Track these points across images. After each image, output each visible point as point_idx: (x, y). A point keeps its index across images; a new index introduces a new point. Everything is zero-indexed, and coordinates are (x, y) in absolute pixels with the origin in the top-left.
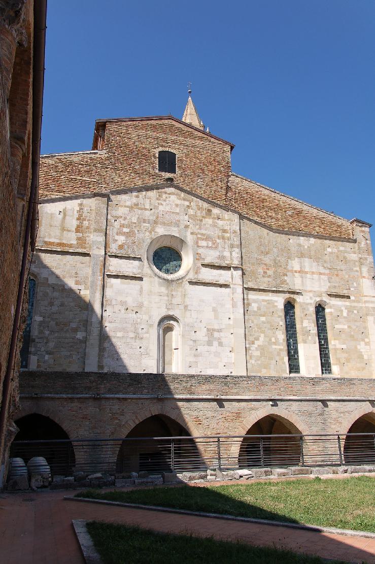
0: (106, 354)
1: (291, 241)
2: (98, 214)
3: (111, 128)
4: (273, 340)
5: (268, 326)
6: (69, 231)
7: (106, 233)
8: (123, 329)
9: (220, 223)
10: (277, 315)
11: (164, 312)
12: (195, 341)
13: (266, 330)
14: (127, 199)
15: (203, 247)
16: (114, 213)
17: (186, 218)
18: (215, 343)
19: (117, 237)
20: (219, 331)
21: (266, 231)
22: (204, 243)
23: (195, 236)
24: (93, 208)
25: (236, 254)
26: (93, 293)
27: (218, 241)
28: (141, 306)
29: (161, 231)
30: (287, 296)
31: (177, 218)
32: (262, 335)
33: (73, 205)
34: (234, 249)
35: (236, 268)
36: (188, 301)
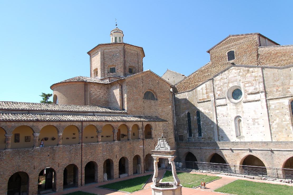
0: (220, 131)
1: (291, 70)
2: (211, 86)
3: (210, 52)
4: (284, 120)
5: (280, 114)
6: (204, 94)
7: (214, 92)
8: (224, 123)
9: (253, 74)
10: (285, 108)
11: (236, 115)
12: (248, 124)
13: (280, 116)
14: (218, 78)
15: (247, 87)
16: (215, 84)
17: (239, 77)
18: (256, 124)
19: (217, 92)
20: (257, 119)
21: (276, 70)
22: (247, 85)
23: (244, 83)
24: (209, 84)
25: (261, 85)
26: (213, 112)
27: (253, 82)
28: (228, 114)
29: (231, 85)
30: (290, 98)
31: (236, 78)
32: (278, 118)
33: (204, 86)
34: (260, 84)
35: (262, 92)
36: (244, 110)
